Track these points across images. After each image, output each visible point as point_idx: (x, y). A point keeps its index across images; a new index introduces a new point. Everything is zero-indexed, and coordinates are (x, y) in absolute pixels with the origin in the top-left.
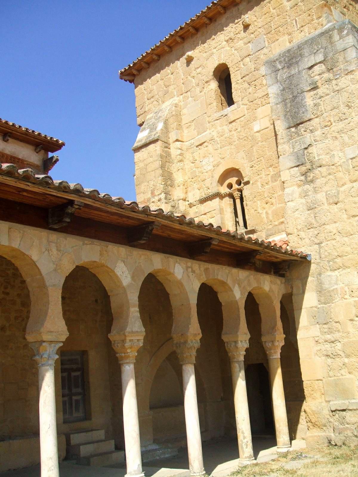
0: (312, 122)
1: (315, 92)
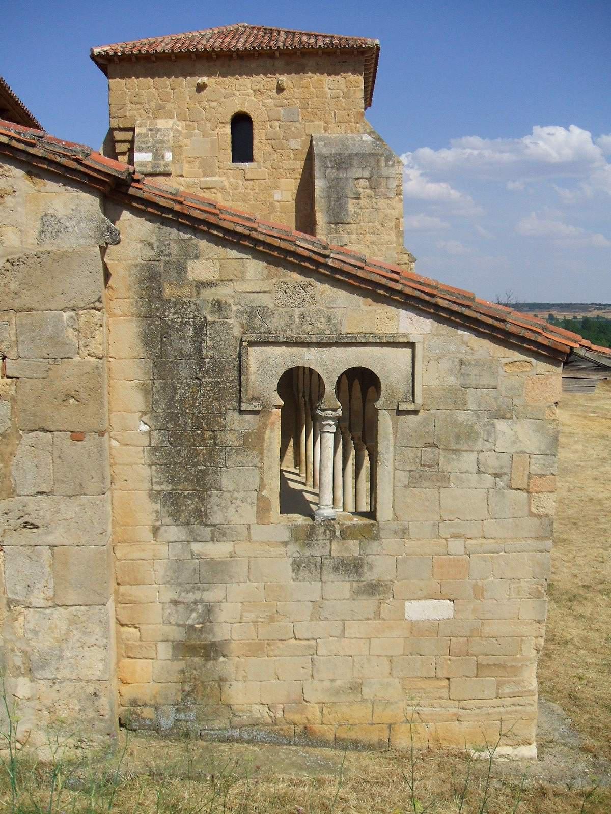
0: (350, 226)
1: (357, 201)
